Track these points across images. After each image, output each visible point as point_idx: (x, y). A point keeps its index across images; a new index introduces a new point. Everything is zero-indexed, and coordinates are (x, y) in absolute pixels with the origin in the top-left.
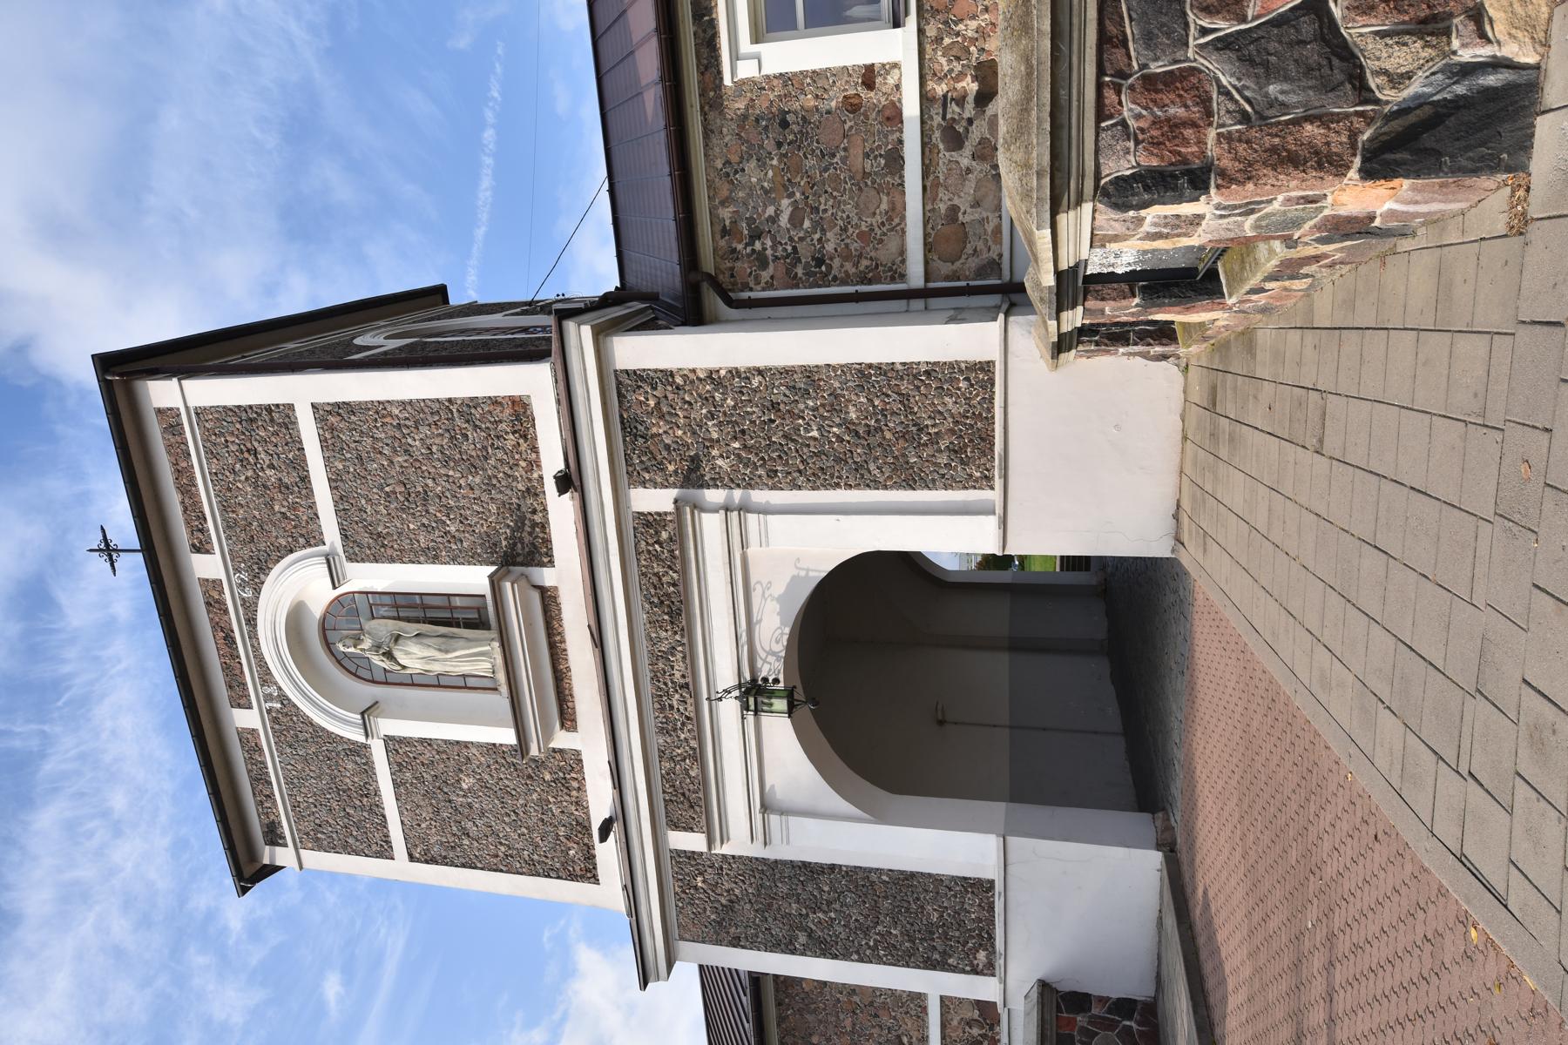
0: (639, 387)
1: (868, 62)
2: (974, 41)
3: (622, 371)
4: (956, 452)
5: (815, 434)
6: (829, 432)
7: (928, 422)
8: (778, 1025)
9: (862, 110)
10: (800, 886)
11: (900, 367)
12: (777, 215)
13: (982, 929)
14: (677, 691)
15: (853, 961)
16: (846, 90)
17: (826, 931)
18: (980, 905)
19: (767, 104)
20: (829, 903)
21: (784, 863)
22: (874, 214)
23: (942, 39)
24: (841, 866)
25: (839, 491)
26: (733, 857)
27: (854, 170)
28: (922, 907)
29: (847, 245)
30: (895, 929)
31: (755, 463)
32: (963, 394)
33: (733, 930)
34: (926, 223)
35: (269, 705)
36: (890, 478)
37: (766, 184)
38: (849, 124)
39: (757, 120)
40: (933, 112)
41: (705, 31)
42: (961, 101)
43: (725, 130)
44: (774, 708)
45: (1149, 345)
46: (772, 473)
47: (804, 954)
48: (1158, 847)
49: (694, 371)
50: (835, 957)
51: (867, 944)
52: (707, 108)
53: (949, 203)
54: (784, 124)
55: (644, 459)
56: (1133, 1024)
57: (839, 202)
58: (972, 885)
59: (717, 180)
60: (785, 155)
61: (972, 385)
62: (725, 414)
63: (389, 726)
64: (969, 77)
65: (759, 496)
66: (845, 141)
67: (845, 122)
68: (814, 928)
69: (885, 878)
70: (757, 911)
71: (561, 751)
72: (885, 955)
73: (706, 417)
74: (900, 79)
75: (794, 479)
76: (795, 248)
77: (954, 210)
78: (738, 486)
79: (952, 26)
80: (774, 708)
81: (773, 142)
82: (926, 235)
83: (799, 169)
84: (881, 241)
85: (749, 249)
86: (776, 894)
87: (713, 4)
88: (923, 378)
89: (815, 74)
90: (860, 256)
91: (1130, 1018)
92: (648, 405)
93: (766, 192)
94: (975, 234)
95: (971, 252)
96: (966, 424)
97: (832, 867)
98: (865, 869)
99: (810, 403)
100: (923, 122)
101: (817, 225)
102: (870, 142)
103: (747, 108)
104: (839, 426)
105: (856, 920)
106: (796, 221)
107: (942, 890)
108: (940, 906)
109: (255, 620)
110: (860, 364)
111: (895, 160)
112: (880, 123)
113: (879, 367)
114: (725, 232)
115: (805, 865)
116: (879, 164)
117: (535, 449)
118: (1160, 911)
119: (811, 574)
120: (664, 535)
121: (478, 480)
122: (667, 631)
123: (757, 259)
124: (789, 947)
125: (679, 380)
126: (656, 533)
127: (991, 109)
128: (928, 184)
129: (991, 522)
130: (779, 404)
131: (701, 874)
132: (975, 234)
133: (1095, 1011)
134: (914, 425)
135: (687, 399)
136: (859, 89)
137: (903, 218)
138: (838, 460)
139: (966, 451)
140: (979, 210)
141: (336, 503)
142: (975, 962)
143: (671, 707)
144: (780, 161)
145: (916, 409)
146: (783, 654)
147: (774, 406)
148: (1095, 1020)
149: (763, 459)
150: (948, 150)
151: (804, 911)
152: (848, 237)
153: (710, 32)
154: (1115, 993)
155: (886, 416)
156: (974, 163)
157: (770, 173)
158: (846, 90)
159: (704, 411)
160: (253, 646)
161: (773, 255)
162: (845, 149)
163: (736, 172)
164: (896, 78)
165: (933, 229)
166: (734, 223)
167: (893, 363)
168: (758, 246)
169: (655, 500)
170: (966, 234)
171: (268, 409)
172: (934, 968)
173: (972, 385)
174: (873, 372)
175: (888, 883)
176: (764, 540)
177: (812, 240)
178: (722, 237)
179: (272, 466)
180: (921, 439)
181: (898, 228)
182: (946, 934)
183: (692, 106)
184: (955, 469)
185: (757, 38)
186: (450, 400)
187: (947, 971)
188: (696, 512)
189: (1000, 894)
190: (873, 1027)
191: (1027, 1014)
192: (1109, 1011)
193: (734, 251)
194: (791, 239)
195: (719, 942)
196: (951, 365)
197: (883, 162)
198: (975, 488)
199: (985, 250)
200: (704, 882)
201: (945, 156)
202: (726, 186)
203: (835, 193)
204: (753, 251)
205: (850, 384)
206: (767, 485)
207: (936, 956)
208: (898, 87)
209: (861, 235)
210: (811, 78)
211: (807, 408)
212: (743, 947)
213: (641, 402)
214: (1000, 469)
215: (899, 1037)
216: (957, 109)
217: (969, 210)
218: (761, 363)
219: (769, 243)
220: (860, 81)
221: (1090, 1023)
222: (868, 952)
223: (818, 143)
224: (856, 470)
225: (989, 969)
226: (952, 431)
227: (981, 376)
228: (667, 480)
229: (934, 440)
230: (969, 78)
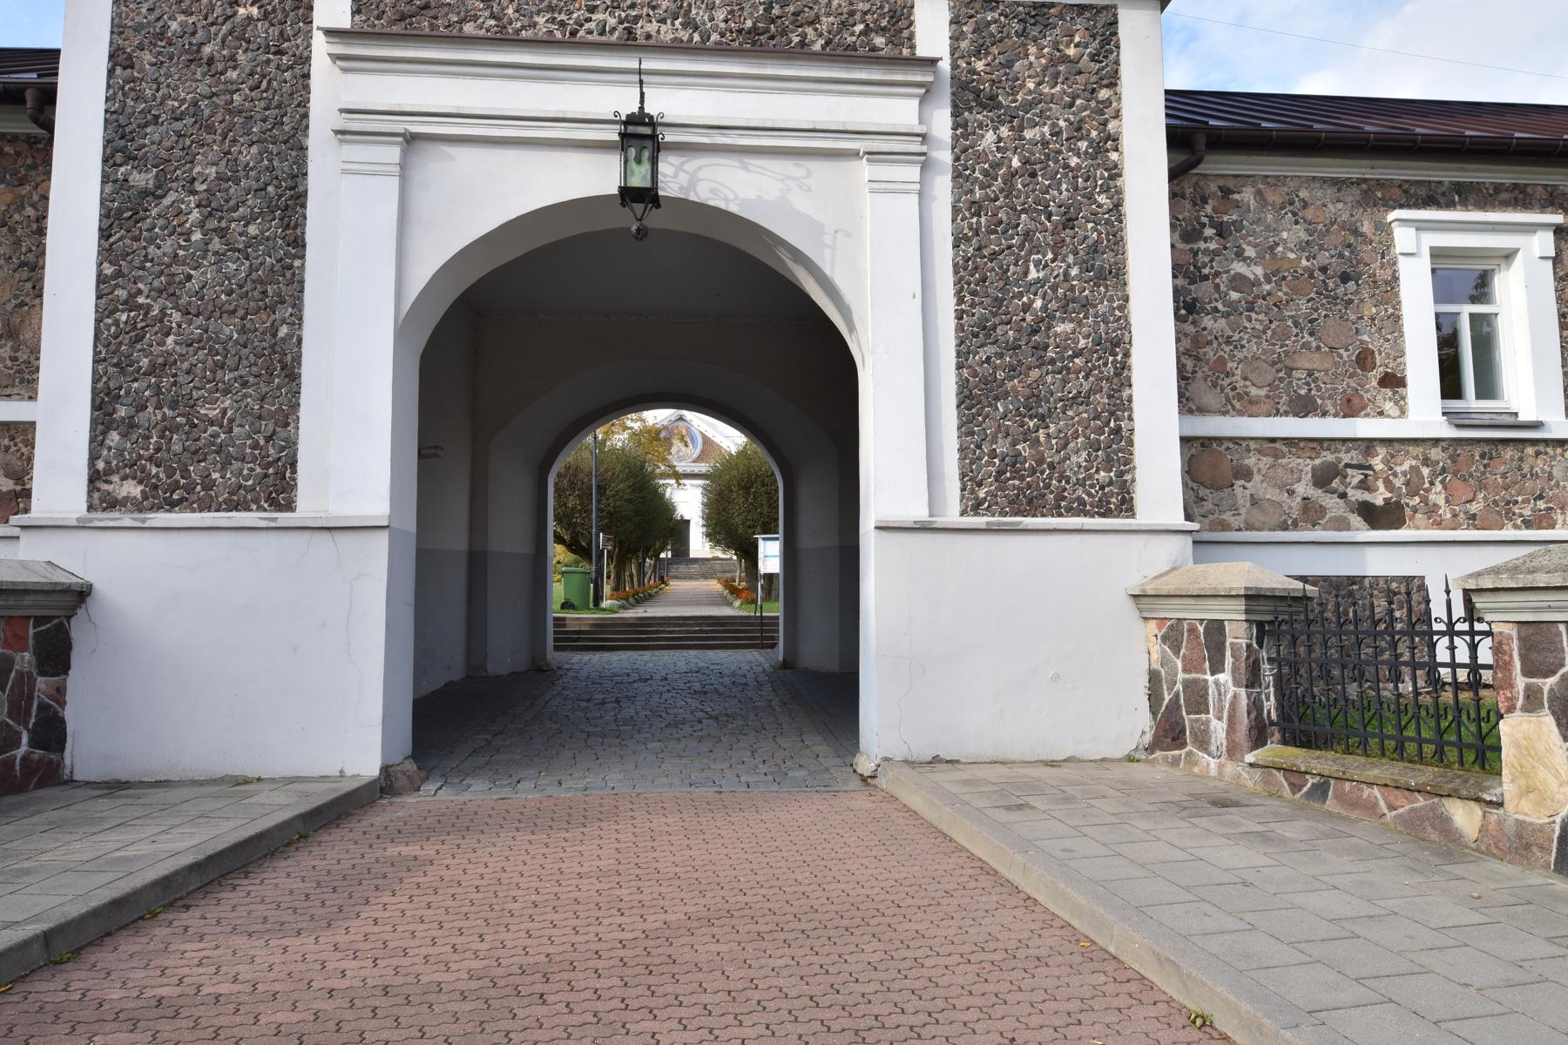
0: (1094, 36)
1: (1409, 380)
2: (1425, 500)
3: (1115, 15)
4: (1013, 465)
5: (1033, 274)
6: (1036, 294)
7: (1052, 428)
9: (1359, 371)
10: (254, 185)
11: (1125, 395)
12: (1245, 260)
13: (189, 489)
14: (621, 22)
15: (100, 265)
16: (1380, 353)
17: (161, 222)
18: (240, 487)
19: (1367, 260)
20: (222, 233)
21: (301, 162)
22: (1245, 379)
23: (1428, 466)
24: (303, 257)
25: (954, 301)
26: (307, 76)
27: (1296, 357)
28: (226, 392)
29: (1209, 343)
30: (176, 343)
31: (989, 186)
32: (1090, 477)
34: (1236, 440)
36: (975, 375)
37: (1280, 249)
38: (1345, 354)
39: (1349, 246)
40: (1354, 453)
41: (1443, 194)
42: (1364, 485)
43: (1340, 205)
44: (633, 165)
45: (1249, 713)
46: (977, 208)
47: (105, 179)
48: (385, 769)
49: (1117, 115)
50: (104, 234)
51: (140, 292)
52: (1364, 186)
53: (1255, 470)
54: (1345, 278)
55: (993, 28)
56: (24, 748)
57: (1259, 337)
59: (1286, 189)
60: (1311, 276)
61: (1102, 488)
62: (1059, 152)
64: (1389, 495)
65: (943, 188)
66: (1327, 349)
67: (1347, 350)
68: (167, 201)
69: (283, 331)
70: (195, 104)
72: (117, 323)
73: (1054, 125)
74: (1389, 416)
75: (968, 240)
76: (1206, 278)
77: (1247, 474)
78: (957, 159)
79: (1440, 478)
80: (633, 165)
81: (1327, 262)
82: (1220, 440)
83: (1296, 291)
84: (1215, 385)
85: (1205, 220)
86: (234, 141)
87: (1470, 208)
88: (1112, 424)
89: (1396, 319)
90: (1198, 359)
91: (33, 743)
92: (1068, 46)
93: (1272, 248)
94: (1221, 499)
95: (1201, 494)
96: (1051, 479)
97: (299, 244)
98: (301, 299)
99: (1074, 272)
100: (1344, 440)
101: (1233, 310)
102: (1325, 379)
103: (1362, 235)
104: (1044, 308)
105: (189, 278)
106: (1238, 282)
107: (267, 426)
108: (231, 421)
110: (1130, 343)
111: (1304, 407)
112: (1345, 391)
113: (1123, 368)
114: (1226, 192)
115: (300, 198)
116: (1300, 388)
118: (259, 779)
119: (828, 252)
120: (879, 41)
122: (726, 21)
123: (1194, 229)
126: (883, 29)
127: (1356, 520)
128: (1277, 445)
129: (920, 513)
130: (1073, 228)
131: (266, 16)
132: (1221, 499)
133: (41, 683)
134: (1049, 409)
135: (1078, 102)
136: (1381, 369)
137: (1241, 413)
138: (998, 302)
139: (1014, 478)
140: (1248, 504)
142: (115, 478)
144: (1306, 269)
145: (1070, 413)
146: (693, 198)
147: (1069, 222)
148: (25, 680)
149: (997, 199)
150: (1313, 469)
151: (201, 187)
152: (1220, 345)
153: (1442, 200)
154: (73, 715)
155: (1060, 373)
156: (1299, 499)
157: (1292, 256)
158: (1380, 353)
159: (1062, 123)
161: (1199, 249)
162: (1318, 348)
163: (1294, 214)
164: (1391, 412)
165: (1227, 449)
166: (1237, 205)
167: (1130, 386)
168: (1209, 232)
170: (1219, 488)
172: (97, 406)
173: (1102, 488)
174: (1119, 358)
175: (274, 335)
176: (879, 187)
177: (1216, 300)
178: (1219, 187)
180: (1031, 418)
181: (1229, 407)
182: (175, 428)
183: (1373, 168)
184: (989, 463)
185: (1437, 254)
187: (93, 429)
188: (923, 91)
189: (275, 520)
191: (24, 565)
192: (43, 707)
193: (1204, 201)
194: (1217, 274)
196: (1128, 462)
197: (1303, 392)
198: (963, 490)
199: (1203, 511)
200: (249, 18)
201: (1307, 465)
202: (1279, 200)
203: (1269, 332)
204: (1204, 225)
205: (1102, 326)
206: (959, 201)
207: (122, 412)
208: (1381, 414)
209: (1222, 361)
210: (1392, 314)
211: (1069, 266)
212: (111, 72)
213: (1072, 36)
214: (999, 524)
216: (1355, 481)
217: (1248, 493)
218: (1129, 208)
219: (1212, 246)
220: (1389, 371)
221: (21, 675)
222: (122, 293)
223: (1325, 316)
224: (984, 328)
225: (101, 499)
226: (1040, 461)
227: (1114, 500)
228: (963, 57)
229: (1027, 436)
230: (1388, 495)
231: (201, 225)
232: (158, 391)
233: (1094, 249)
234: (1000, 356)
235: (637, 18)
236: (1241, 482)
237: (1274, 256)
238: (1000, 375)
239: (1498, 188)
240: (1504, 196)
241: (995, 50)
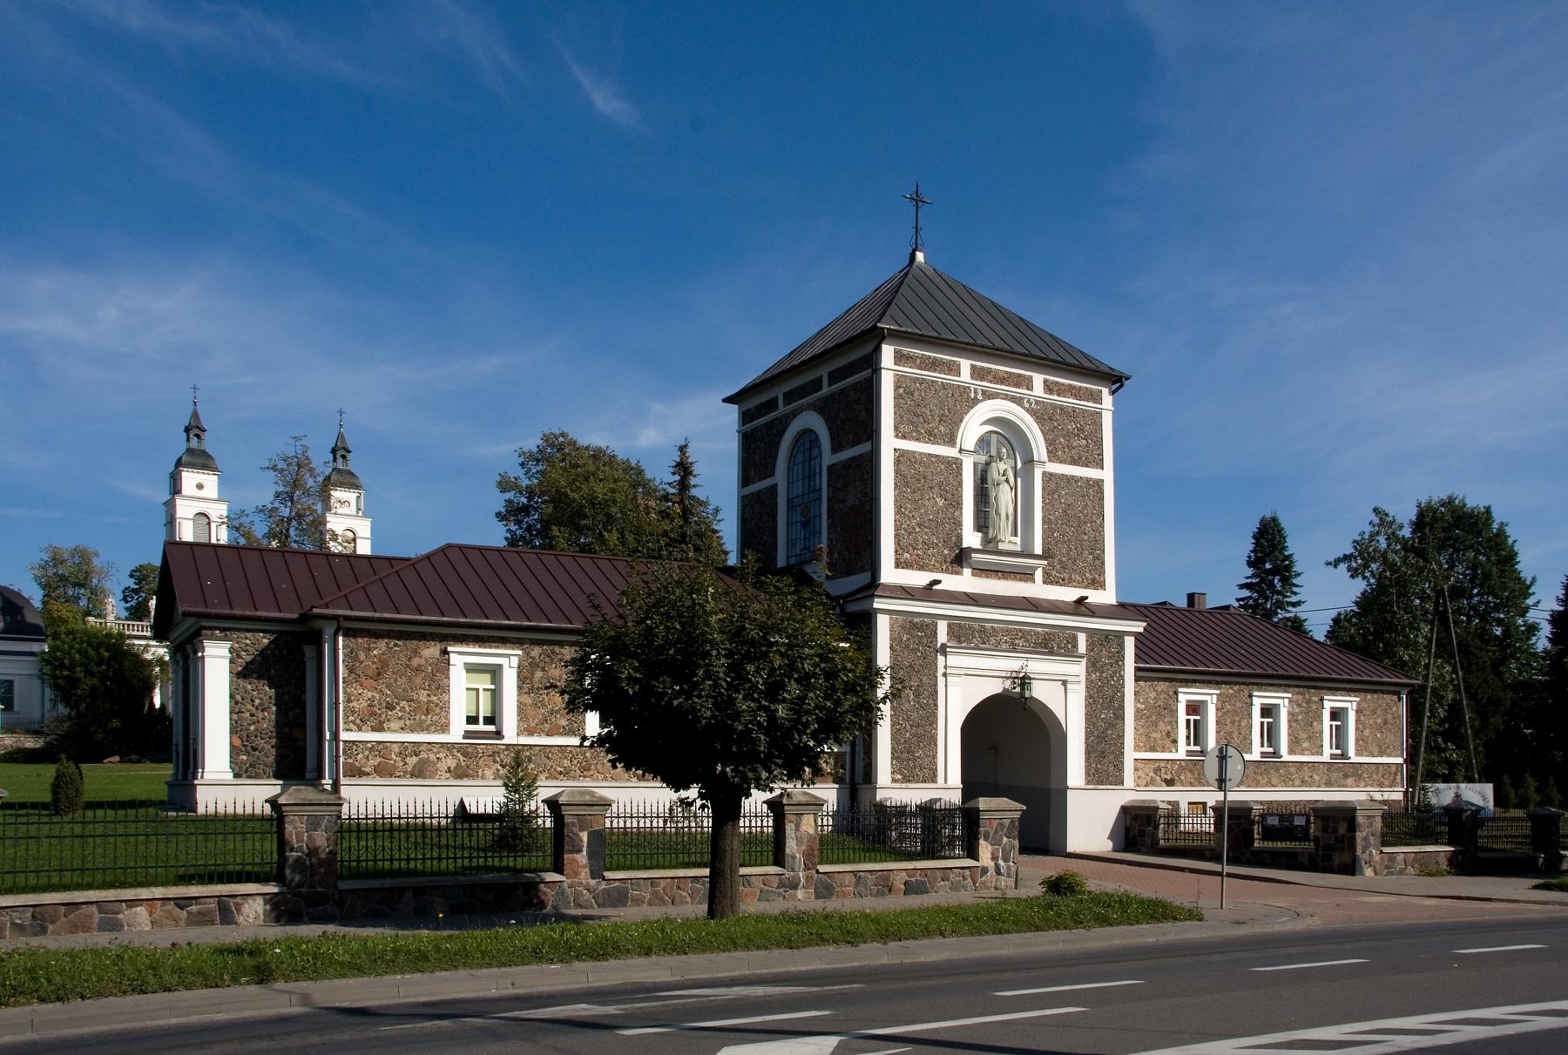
20: (918, 702)
42: (1165, 773)
54: (1165, 709)
127: (1163, 784)
225: (894, 781)
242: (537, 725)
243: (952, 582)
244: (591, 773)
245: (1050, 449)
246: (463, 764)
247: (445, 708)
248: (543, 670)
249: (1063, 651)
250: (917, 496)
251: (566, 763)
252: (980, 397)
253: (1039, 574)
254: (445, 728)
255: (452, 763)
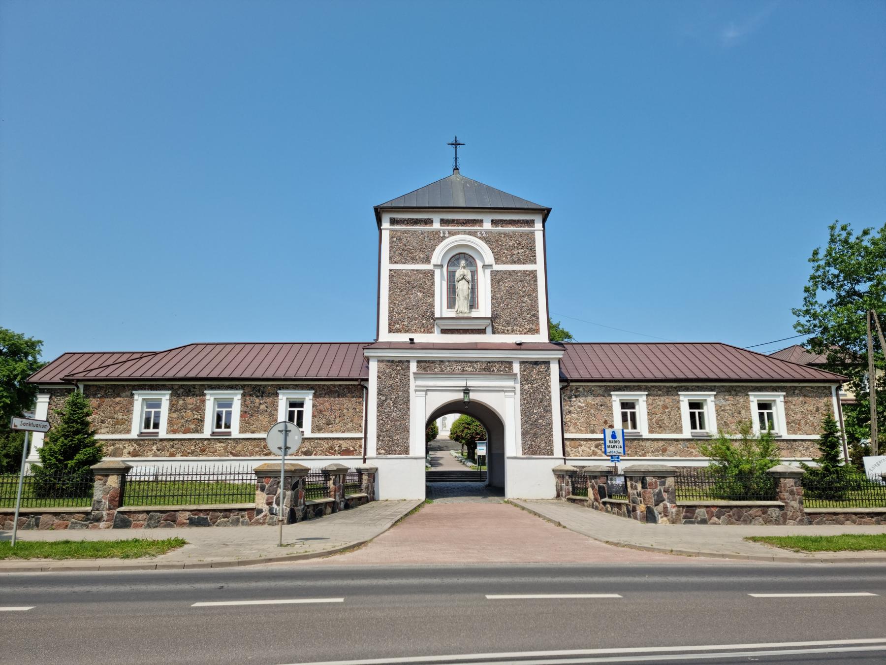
5: (535, 411)
8: (332, 385)
20: (396, 407)
21: (409, 395)
26: (409, 379)
33: (383, 377)
35: (442, 232)
46: (525, 399)
50: (378, 408)
54: (601, 406)
58: (407, 448)
63: (437, 272)
71: (434, 327)
97: (409, 409)
99: (542, 411)
106: (579, 407)
109: (470, 235)
113: (551, 428)
114: (577, 388)
115: (409, 401)
117: (525, 333)
120: (507, 369)
121: (516, 316)
124: (380, 393)
125: (547, 378)
131: (402, 369)
141: (508, 271)
143: (457, 366)
151: (393, 399)
160: (462, 232)
166: (579, 391)
168: (573, 397)
169: (516, 368)
171: (535, 256)
179: (518, 253)
186: (538, 311)
190: (335, 416)
195: (378, 372)
215: (332, 424)
218: (552, 399)
226: (536, 445)
229: (533, 441)
231: (393, 406)
232: (387, 434)
233: (546, 406)
234: (529, 426)
235: (464, 367)
236: (580, 447)
237: (587, 402)
238: (529, 430)
239: (634, 386)
240: (636, 388)
241: (528, 370)
242: (178, 428)
243: (420, 338)
244: (206, 453)
245: (496, 257)
246: (137, 449)
247: (130, 421)
248: (184, 400)
249: (502, 372)
250: (404, 293)
251: (193, 448)
252: (447, 235)
253: (489, 330)
254: (128, 431)
255: (131, 449)
